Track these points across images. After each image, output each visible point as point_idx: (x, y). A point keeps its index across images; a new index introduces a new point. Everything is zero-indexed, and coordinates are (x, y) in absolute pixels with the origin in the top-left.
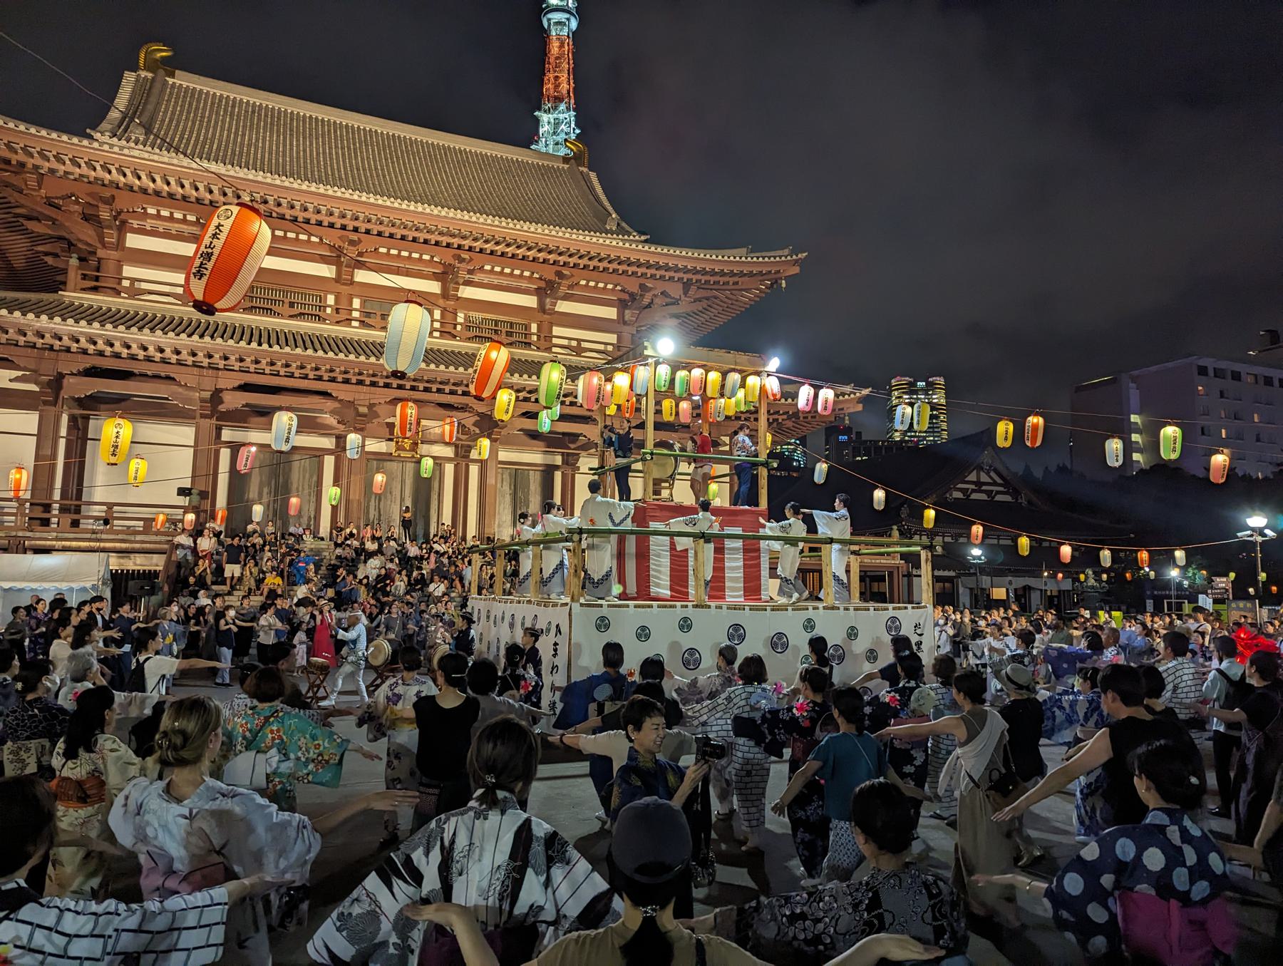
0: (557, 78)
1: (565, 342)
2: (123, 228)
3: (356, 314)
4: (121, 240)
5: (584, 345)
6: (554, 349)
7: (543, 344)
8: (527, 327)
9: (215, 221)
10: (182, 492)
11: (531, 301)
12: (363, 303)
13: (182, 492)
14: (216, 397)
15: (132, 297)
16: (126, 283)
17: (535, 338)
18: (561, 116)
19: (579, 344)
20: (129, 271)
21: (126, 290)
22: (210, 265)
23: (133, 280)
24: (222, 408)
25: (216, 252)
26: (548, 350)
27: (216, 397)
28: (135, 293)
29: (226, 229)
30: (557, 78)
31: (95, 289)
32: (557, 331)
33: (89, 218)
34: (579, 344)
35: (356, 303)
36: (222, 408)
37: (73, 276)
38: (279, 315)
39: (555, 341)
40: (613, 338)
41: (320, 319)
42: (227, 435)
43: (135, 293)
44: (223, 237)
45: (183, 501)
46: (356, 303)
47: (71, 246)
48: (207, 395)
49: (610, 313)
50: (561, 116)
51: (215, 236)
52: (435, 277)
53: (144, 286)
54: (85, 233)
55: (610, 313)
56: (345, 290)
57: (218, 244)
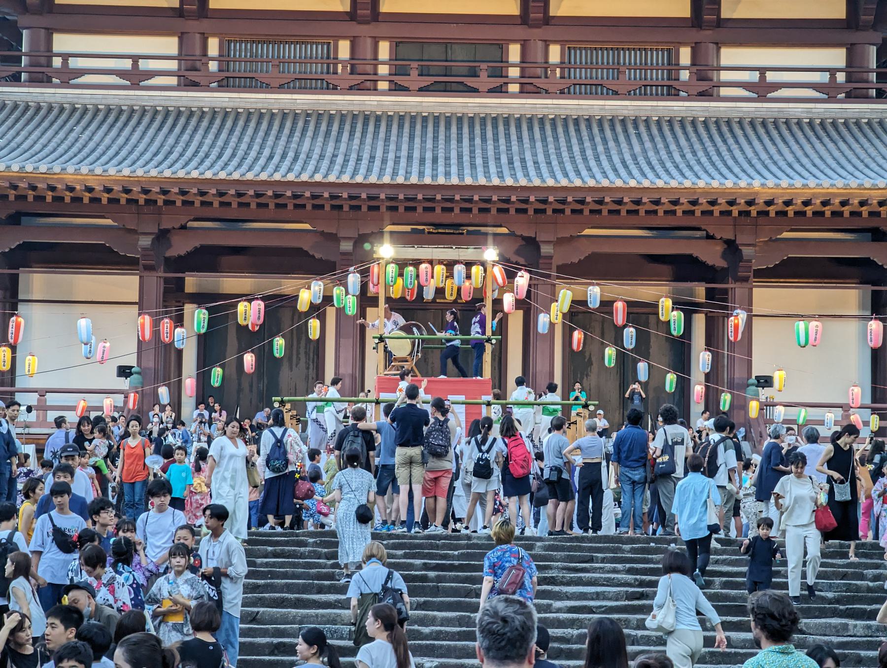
1: (745, 76)
3: (383, 70)
5: (771, 77)
6: (724, 92)
7: (704, 86)
10: (124, 372)
13: (124, 372)
15: (65, 84)
16: (57, 62)
17: (685, 75)
19: (763, 77)
20: (63, 42)
21: (58, 72)
23: (66, 57)
28: (68, 76)
32: (730, 56)
34: (763, 77)
35: (384, 50)
39: (725, 76)
40: (836, 57)
42: (192, 282)
43: (68, 76)
45: (124, 384)
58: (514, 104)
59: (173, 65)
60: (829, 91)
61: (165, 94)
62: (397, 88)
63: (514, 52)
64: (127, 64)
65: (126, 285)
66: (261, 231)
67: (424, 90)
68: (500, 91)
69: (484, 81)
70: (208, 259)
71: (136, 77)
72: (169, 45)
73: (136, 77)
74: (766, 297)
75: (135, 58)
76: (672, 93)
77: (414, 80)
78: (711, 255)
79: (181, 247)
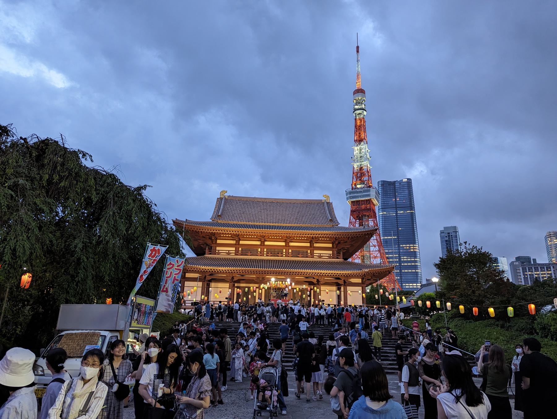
0: (360, 133)
2: (216, 239)
4: (216, 241)
8: (307, 252)
10: (226, 298)
13: (226, 298)
18: (362, 147)
20: (218, 248)
30: (360, 133)
31: (211, 254)
32: (315, 252)
33: (210, 238)
35: (265, 250)
37: (207, 251)
38: (248, 255)
40: (331, 252)
41: (257, 255)
42: (236, 285)
43: (219, 254)
45: (226, 300)
46: (265, 250)
47: (207, 245)
49: (330, 245)
50: (362, 147)
52: (284, 241)
54: (209, 242)
55: (330, 245)
56: (262, 247)
58: (284, 258)
60: (330, 257)
63: (284, 251)
65: (227, 285)
66: (247, 276)
68: (282, 256)
69: (280, 255)
70: (239, 281)
71: (229, 254)
72: (234, 249)
74: (323, 288)
76: (307, 257)
77: (269, 254)
78: (315, 281)
79: (235, 279)
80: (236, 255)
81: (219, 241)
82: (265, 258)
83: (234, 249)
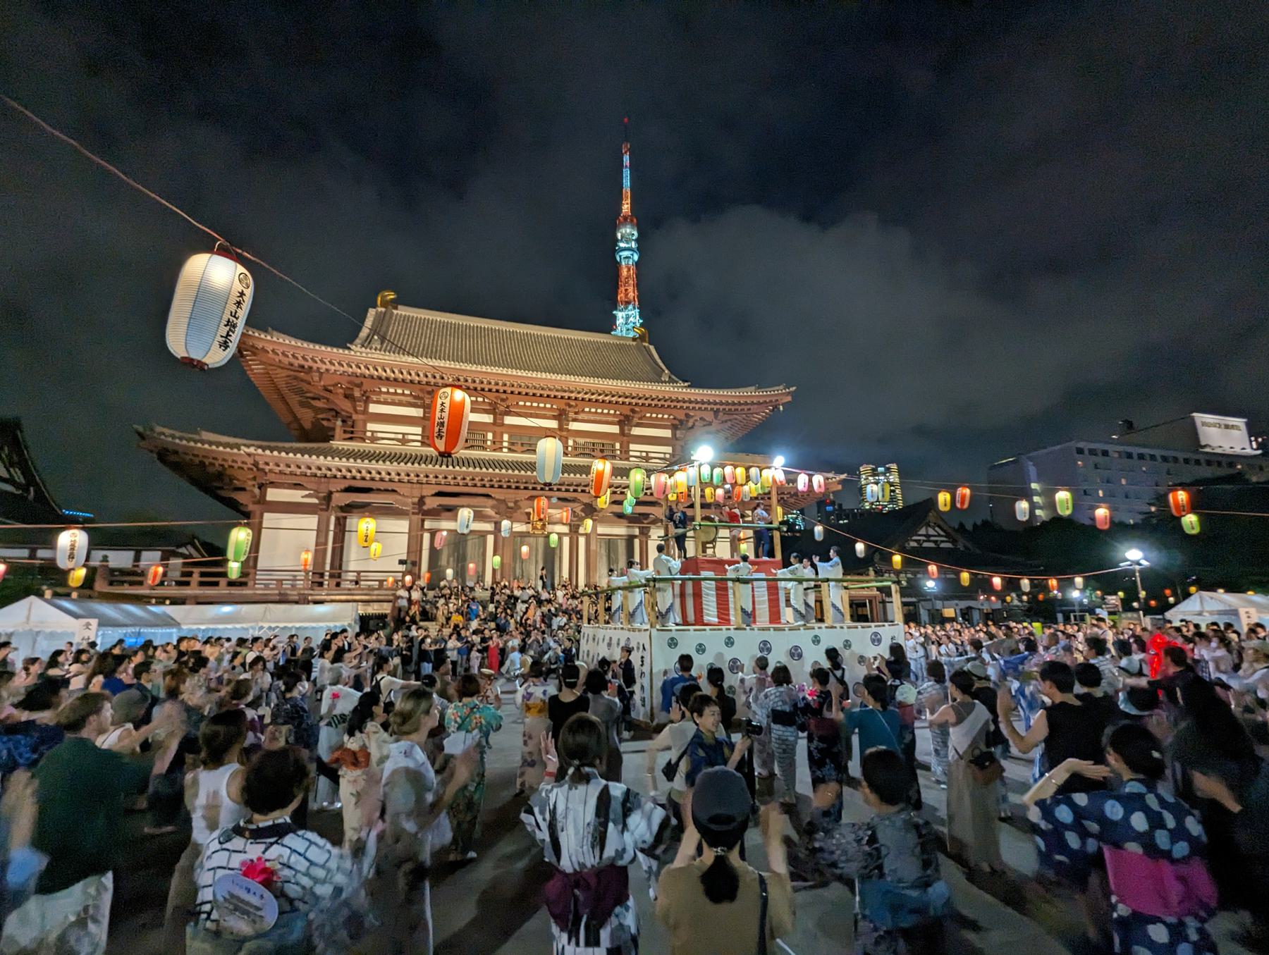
2: (367, 401)
3: (505, 444)
4: (366, 407)
7: (624, 456)
8: (613, 446)
9: (439, 402)
10: (401, 562)
11: (615, 429)
12: (510, 437)
13: (401, 562)
14: (421, 501)
16: (369, 434)
20: (371, 426)
21: (369, 438)
22: (444, 430)
23: (373, 432)
24: (425, 508)
25: (446, 420)
26: (627, 459)
27: (421, 501)
28: (374, 439)
29: (447, 405)
31: (351, 439)
32: (632, 447)
35: (506, 437)
36: (425, 508)
37: (338, 431)
40: (669, 449)
41: (484, 449)
43: (374, 439)
44: (447, 410)
45: (403, 568)
46: (506, 437)
48: (416, 500)
49: (667, 433)
51: (442, 411)
52: (554, 418)
53: (380, 435)
54: (346, 405)
55: (667, 433)
56: (497, 429)
57: (446, 415)
59: (419, 438)
61: (415, 448)
62: (510, 450)
64: (400, 436)
67: (523, 452)
71: (404, 441)
72: (419, 430)
73: (404, 441)
75: (404, 434)
80: (423, 444)
81: (373, 408)
82: (505, 455)
83: (419, 430)
